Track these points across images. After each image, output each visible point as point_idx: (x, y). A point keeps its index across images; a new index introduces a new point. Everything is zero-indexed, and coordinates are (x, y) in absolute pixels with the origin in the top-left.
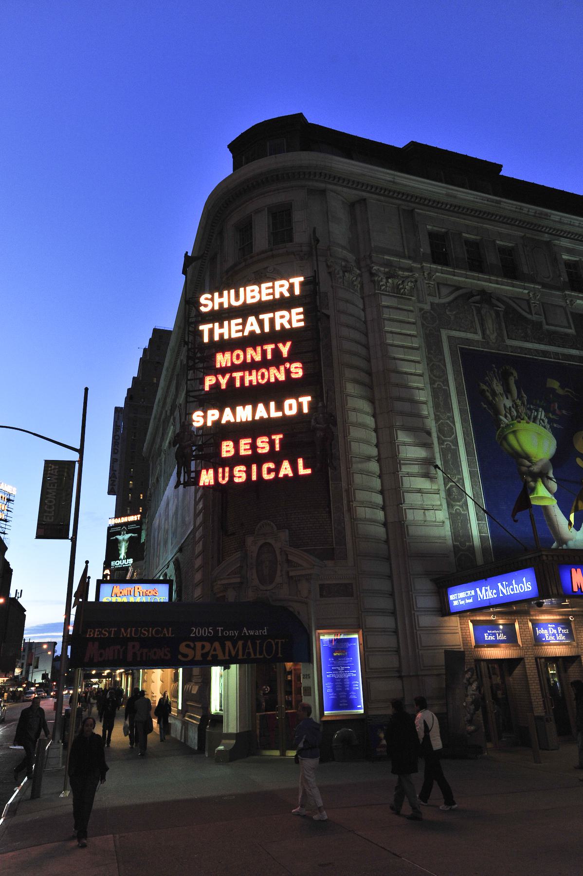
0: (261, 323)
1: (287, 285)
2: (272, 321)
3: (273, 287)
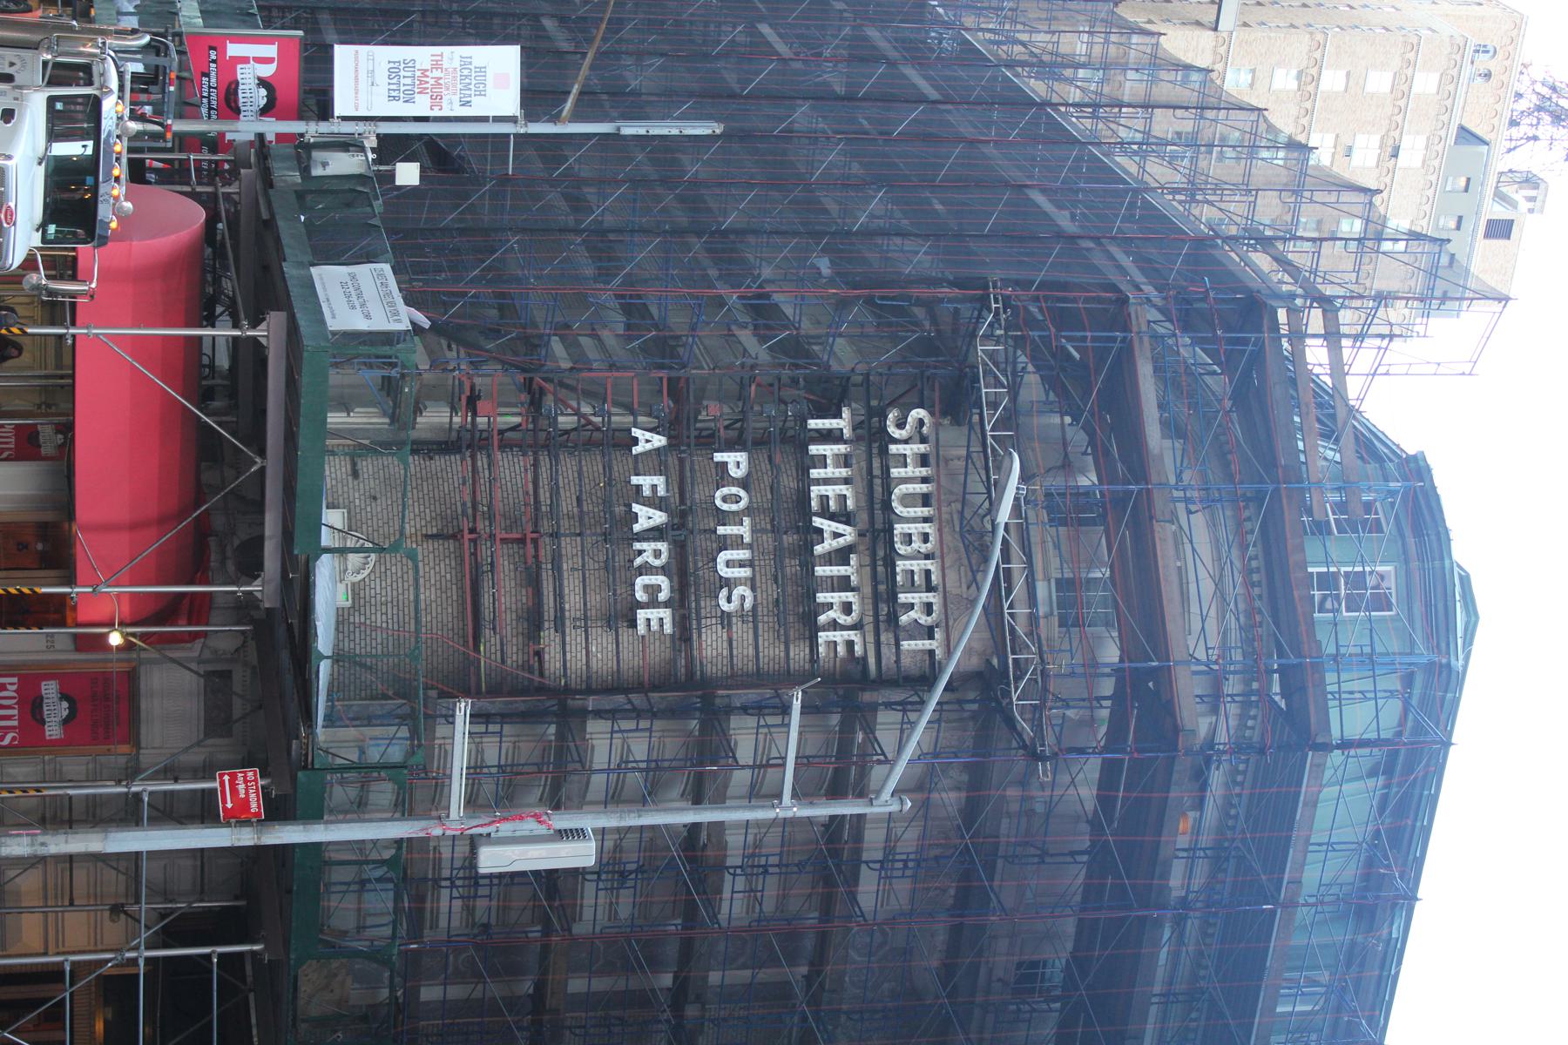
0: (841, 556)
1: (925, 620)
2: (843, 584)
3: (930, 588)
